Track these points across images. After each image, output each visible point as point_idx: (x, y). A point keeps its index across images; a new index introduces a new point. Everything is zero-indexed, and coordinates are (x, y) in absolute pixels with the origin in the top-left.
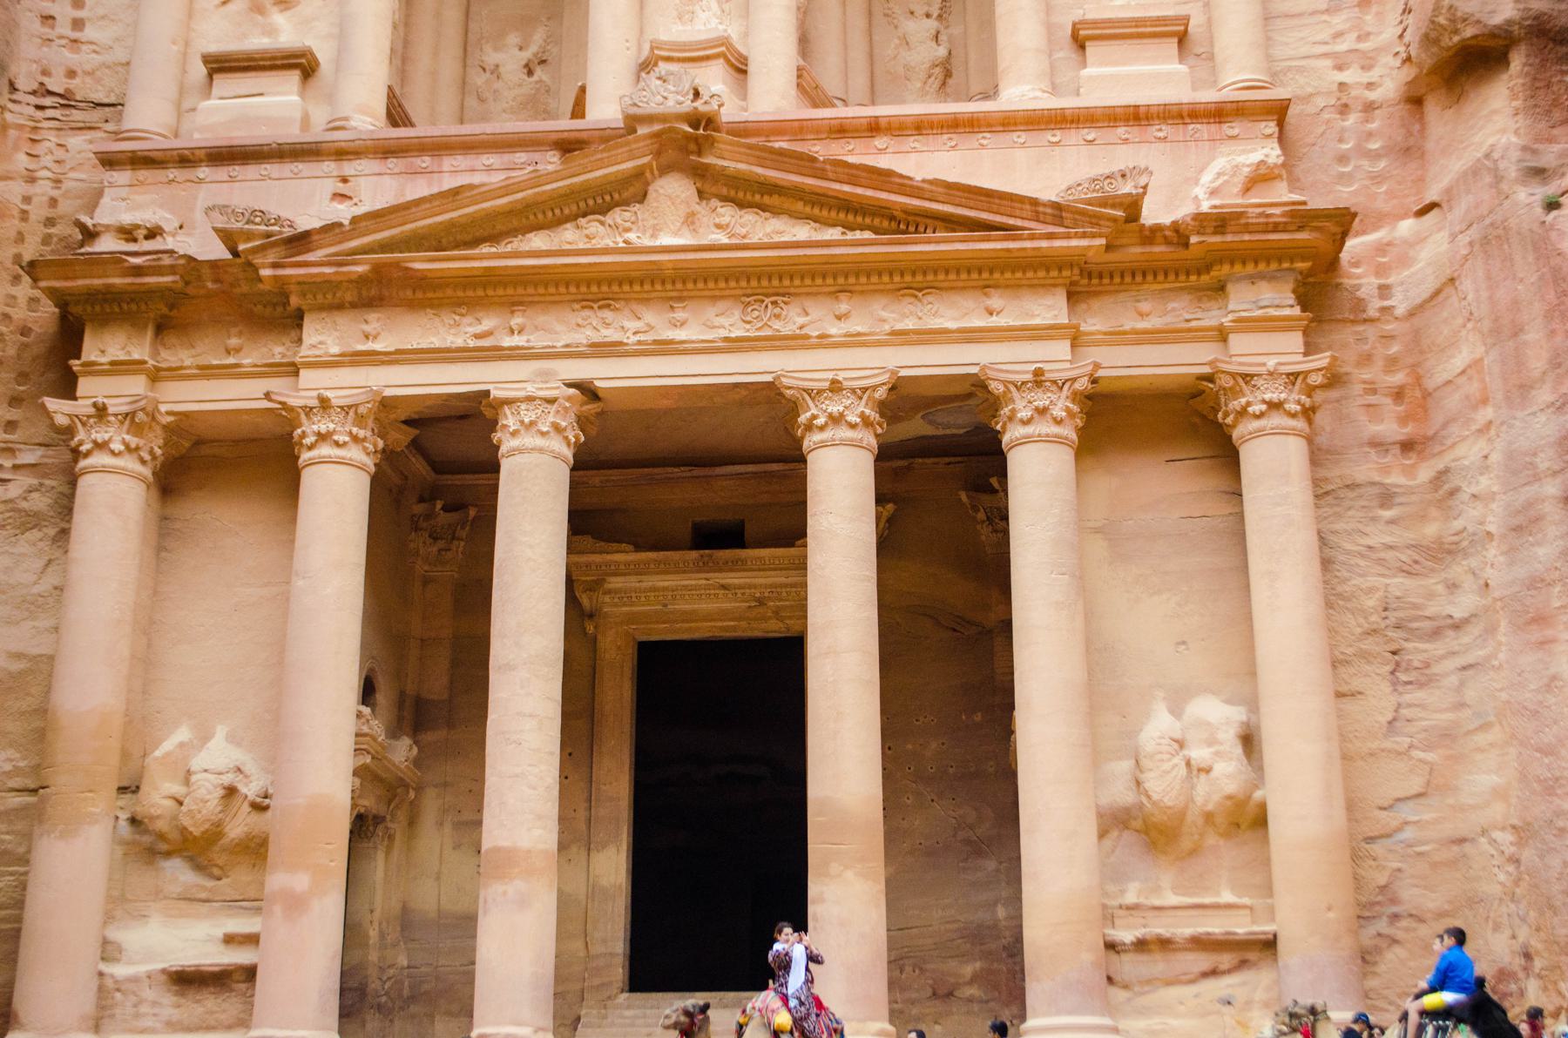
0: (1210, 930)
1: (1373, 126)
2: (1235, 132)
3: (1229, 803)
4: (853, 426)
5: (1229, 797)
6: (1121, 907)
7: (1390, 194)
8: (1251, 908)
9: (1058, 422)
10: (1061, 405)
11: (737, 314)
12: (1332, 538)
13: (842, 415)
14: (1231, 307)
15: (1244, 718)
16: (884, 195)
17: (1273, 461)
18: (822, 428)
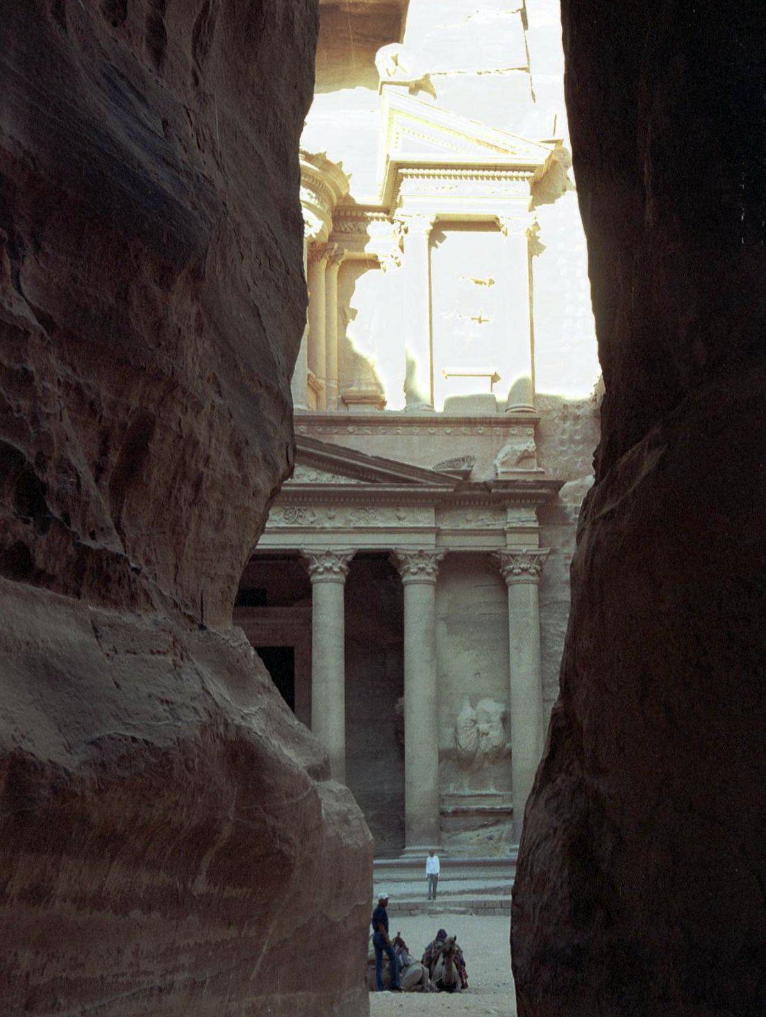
0: (485, 807)
1: (578, 427)
2: (516, 432)
3: (495, 749)
4: (336, 573)
5: (495, 747)
6: (446, 795)
7: (582, 461)
8: (502, 796)
9: (429, 574)
10: (430, 566)
11: (282, 514)
12: (547, 627)
13: (331, 568)
14: (508, 520)
15: (504, 710)
16: (354, 462)
17: (523, 594)
18: (321, 574)
